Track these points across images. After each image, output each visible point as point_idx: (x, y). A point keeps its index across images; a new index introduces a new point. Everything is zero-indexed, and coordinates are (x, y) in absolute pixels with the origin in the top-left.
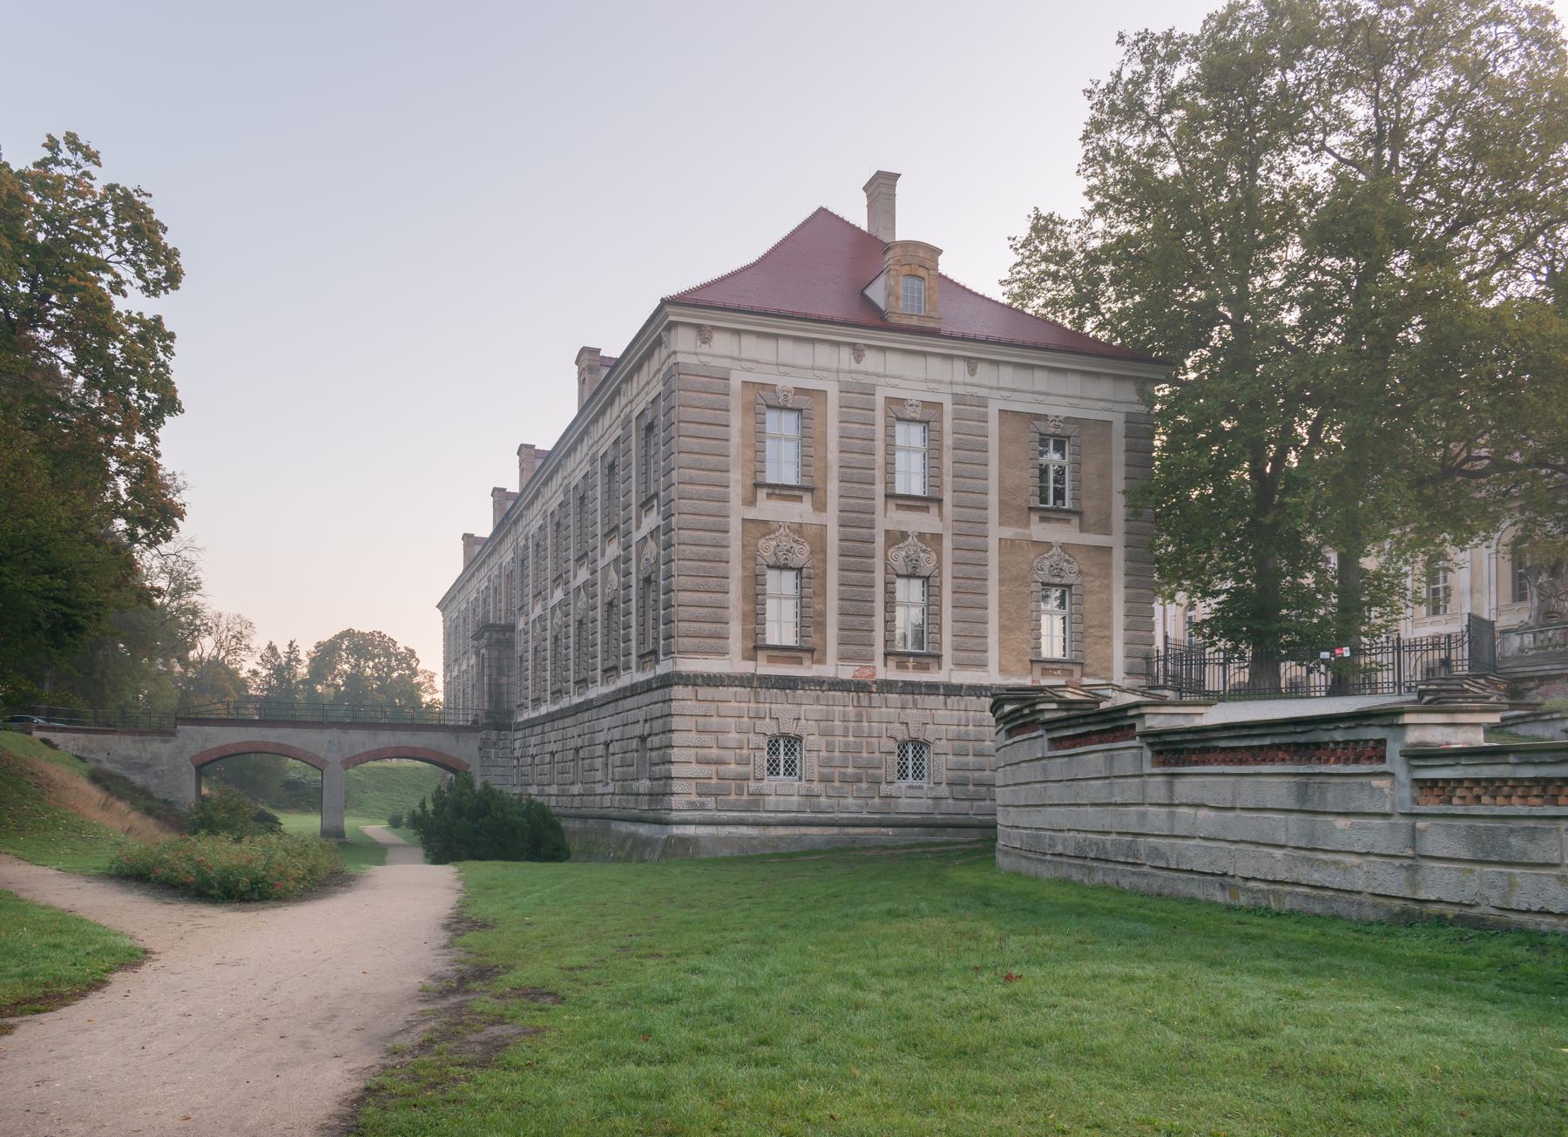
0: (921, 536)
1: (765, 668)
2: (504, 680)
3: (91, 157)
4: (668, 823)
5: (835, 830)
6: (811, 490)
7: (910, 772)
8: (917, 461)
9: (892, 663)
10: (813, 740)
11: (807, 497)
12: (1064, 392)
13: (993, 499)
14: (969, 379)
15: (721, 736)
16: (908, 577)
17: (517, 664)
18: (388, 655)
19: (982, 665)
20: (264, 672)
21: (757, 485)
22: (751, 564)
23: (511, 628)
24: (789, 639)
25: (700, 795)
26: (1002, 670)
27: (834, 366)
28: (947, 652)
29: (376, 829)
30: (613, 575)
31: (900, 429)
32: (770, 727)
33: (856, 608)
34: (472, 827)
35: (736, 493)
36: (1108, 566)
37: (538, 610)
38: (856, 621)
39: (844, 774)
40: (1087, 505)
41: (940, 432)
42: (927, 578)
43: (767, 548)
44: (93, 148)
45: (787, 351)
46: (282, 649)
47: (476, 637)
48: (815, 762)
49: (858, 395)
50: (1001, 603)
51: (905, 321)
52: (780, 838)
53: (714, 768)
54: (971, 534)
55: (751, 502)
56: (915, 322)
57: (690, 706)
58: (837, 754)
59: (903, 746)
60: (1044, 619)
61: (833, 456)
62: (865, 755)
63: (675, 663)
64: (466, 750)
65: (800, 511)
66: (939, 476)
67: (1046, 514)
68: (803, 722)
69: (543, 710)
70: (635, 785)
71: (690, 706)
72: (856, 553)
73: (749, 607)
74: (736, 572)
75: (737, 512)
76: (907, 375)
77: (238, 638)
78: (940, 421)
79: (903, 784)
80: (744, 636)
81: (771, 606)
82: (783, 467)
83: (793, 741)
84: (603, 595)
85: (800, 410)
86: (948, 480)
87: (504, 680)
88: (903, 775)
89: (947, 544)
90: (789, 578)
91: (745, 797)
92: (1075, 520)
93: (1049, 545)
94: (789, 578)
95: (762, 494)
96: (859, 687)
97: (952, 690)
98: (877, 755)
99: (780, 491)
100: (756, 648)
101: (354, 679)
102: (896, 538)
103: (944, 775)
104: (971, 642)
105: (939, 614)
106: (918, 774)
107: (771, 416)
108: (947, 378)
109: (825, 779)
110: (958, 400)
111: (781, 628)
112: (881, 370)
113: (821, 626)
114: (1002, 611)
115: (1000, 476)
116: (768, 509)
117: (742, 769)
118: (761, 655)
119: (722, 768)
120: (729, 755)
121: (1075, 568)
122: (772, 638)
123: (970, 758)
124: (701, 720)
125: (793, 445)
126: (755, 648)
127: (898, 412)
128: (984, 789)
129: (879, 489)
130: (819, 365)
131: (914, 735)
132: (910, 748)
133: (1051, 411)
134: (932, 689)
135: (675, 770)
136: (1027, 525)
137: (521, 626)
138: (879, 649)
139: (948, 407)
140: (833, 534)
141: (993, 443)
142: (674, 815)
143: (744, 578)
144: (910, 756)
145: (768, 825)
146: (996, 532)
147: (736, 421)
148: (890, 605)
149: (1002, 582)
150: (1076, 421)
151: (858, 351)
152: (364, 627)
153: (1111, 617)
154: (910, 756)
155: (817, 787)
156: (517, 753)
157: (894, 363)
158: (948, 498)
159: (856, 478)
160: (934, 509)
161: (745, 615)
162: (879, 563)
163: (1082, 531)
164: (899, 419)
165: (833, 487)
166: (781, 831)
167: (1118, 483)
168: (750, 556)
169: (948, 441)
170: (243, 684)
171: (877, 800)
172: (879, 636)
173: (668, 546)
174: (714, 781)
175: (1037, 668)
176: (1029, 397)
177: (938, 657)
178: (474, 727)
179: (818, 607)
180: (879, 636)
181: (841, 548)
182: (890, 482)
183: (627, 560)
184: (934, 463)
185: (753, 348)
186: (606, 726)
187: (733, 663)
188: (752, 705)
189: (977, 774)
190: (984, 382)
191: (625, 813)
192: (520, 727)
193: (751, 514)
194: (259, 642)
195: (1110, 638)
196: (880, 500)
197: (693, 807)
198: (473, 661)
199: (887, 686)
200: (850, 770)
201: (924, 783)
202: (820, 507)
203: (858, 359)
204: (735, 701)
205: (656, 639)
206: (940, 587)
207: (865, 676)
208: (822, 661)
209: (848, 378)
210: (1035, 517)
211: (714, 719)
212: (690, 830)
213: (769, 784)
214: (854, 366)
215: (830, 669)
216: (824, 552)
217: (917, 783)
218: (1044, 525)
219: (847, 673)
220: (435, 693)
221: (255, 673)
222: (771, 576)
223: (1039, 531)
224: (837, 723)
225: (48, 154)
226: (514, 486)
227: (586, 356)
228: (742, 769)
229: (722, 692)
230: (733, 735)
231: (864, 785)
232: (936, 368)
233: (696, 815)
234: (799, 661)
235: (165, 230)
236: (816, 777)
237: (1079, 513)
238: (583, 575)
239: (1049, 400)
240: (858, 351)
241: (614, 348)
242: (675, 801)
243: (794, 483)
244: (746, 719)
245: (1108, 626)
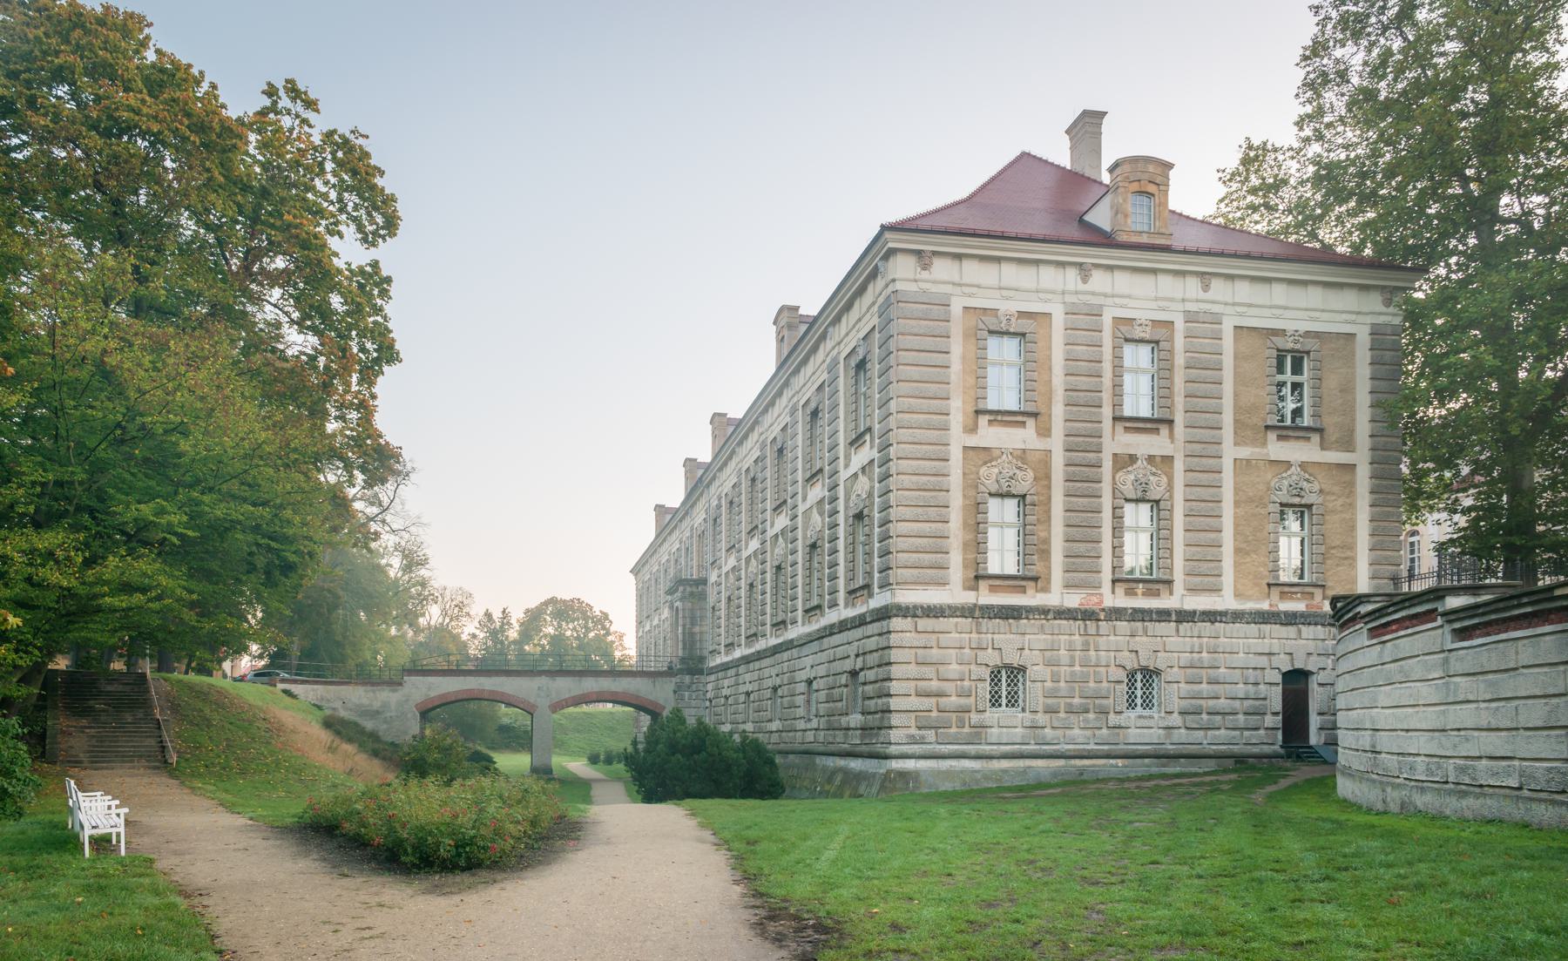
0: (1151, 459)
1: (986, 598)
2: (697, 629)
3: (311, 104)
4: (887, 757)
5: (1062, 762)
6: (1035, 415)
7: (1139, 701)
8: (1145, 383)
9: (1120, 589)
10: (1037, 671)
11: (1031, 422)
12: (1304, 305)
13: (1228, 419)
14: (1202, 295)
15: (941, 668)
16: (1137, 501)
17: (709, 614)
18: (586, 618)
19: (1216, 590)
20: (482, 635)
21: (978, 412)
22: (972, 493)
23: (704, 582)
24: (1011, 568)
25: (919, 728)
26: (1238, 595)
27: (1060, 287)
28: (1178, 576)
29: (578, 766)
30: (816, 518)
31: (1128, 350)
32: (992, 658)
33: (1082, 534)
34: (687, 764)
35: (957, 420)
36: (1350, 486)
37: (732, 562)
38: (1081, 548)
39: (1070, 705)
40: (1328, 421)
41: (1171, 351)
42: (1157, 502)
43: (989, 476)
44: (312, 96)
45: (1010, 274)
46: (497, 615)
47: (670, 592)
48: (1040, 693)
49: (1085, 317)
50: (1236, 526)
51: (1135, 239)
52: (1005, 771)
53: (933, 700)
54: (1204, 454)
55: (972, 429)
56: (1144, 239)
57: (910, 638)
58: (1062, 684)
59: (1131, 675)
60: (1283, 541)
61: (1058, 380)
62: (1092, 684)
63: (893, 595)
64: (662, 694)
65: (1024, 437)
66: (1170, 397)
67: (1284, 433)
68: (1027, 651)
69: (737, 654)
70: (844, 720)
71: (910, 638)
72: (1083, 477)
73: (970, 536)
74: (956, 500)
75: (958, 440)
76: (1133, 294)
77: (460, 606)
78: (1171, 340)
79: (1132, 714)
80: (965, 567)
81: (993, 534)
82: (1004, 392)
83: (1016, 672)
84: (805, 538)
85: (1023, 335)
86: (1179, 401)
87: (697, 629)
88: (1131, 704)
89: (1179, 466)
90: (1011, 505)
91: (967, 730)
92: (1316, 438)
93: (1288, 464)
94: (1011, 505)
95: (983, 420)
96: (1088, 615)
97: (1184, 617)
98: (1105, 684)
99: (1001, 417)
100: (978, 577)
101: (557, 640)
102: (1124, 461)
103: (1176, 704)
104: (1204, 567)
105: (1170, 538)
106: (1147, 704)
107: (993, 342)
108: (1180, 296)
109: (1050, 711)
110: (1190, 317)
111: (1002, 556)
112: (1108, 290)
113: (1045, 554)
114: (1237, 533)
115: (1236, 395)
116: (990, 436)
117: (963, 701)
118: (983, 584)
119: (942, 700)
120: (949, 687)
121: (1316, 487)
122: (993, 568)
123: (1204, 686)
124: (920, 651)
125: (1015, 371)
126: (977, 578)
127: (1126, 333)
128: (1219, 718)
129: (1107, 412)
130: (1043, 287)
131: (1144, 663)
132: (1139, 677)
133: (1290, 326)
134: (1163, 615)
135: (894, 703)
136: (1264, 444)
137: (713, 578)
138: (1107, 576)
139: (1180, 326)
141: (1228, 361)
142: (893, 749)
143: (965, 507)
144: (1139, 685)
145: (991, 757)
146: (1231, 452)
147: (957, 348)
148: (1118, 530)
149: (1237, 504)
150: (1317, 335)
151: (1084, 270)
152: (565, 595)
153: (1354, 537)
154: (1139, 685)
155: (1041, 718)
156: (709, 695)
157: (1123, 282)
158: (1179, 419)
159: (1083, 402)
160: (1164, 430)
161: (966, 545)
163: (1323, 448)
164: (1127, 340)
165: (1058, 411)
166: (1005, 764)
167: (1363, 398)
168: (971, 482)
169: (1180, 360)
170: (465, 645)
171: (1104, 731)
172: (1106, 562)
173: (886, 477)
174: (934, 714)
175: (1275, 591)
176: (1267, 312)
177: (1169, 582)
178: (670, 672)
179: (1043, 534)
180: (1106, 562)
181: (1066, 472)
182: (1117, 405)
183: (834, 500)
184: (1164, 383)
185: (974, 272)
186: (809, 664)
187: (954, 593)
188: (974, 635)
189: (1211, 703)
190: (1219, 298)
191: (832, 748)
192: (712, 671)
193: (973, 441)
194: (477, 610)
195: (1354, 559)
196: (1107, 423)
197: (913, 740)
198: (666, 613)
199: (1116, 614)
200: (1077, 701)
201: (1154, 712)
202: (1045, 432)
203: (1085, 280)
204: (956, 631)
205: (869, 574)
206: (1171, 511)
207: (1092, 603)
208: (1046, 589)
209: (1073, 299)
210: (1272, 436)
211: (935, 651)
212: (910, 764)
213: (992, 716)
214: (1081, 287)
215: (1056, 597)
216: (1048, 477)
217: (1147, 712)
218: (1281, 444)
219: (1073, 600)
220: (627, 644)
221: (474, 636)
222: (993, 505)
223: (1277, 449)
224: (1062, 652)
225: (267, 102)
226: (705, 456)
227: (786, 313)
228: (963, 701)
229: (943, 624)
230: (954, 666)
231: (1091, 716)
232: (1167, 285)
233: (916, 749)
234: (1023, 590)
235: (382, 173)
236: (1040, 708)
237: (1320, 431)
238: (782, 521)
239: (1288, 314)
240: (1084, 270)
241: (811, 308)
242: (894, 735)
243: (1015, 408)
244: (967, 651)
245: (1352, 547)
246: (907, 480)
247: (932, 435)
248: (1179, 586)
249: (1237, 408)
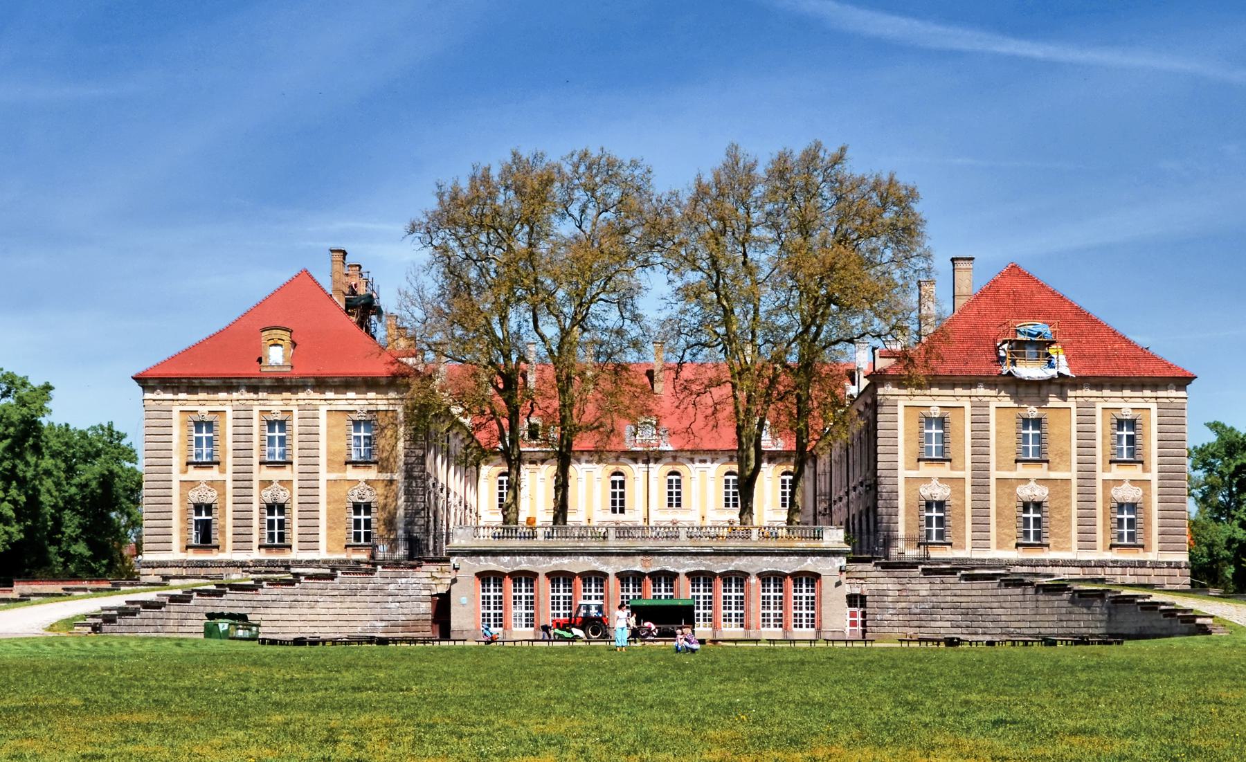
0: (280, 482)
1: (192, 556)
13: (323, 460)
26: (329, 551)
43: (194, 496)
54: (309, 478)
55: (186, 472)
65: (213, 474)
72: (243, 495)
75: (177, 477)
89: (296, 485)
93: (358, 481)
102: (266, 484)
129: (256, 460)
140: (230, 485)
141: (323, 430)
143: (181, 511)
146: (324, 475)
149: (328, 503)
158: (296, 461)
160: (288, 466)
161: (182, 530)
162: (255, 500)
168: (184, 498)
193: (185, 477)
202: (223, 471)
208: (224, 551)
210: (350, 466)
223: (352, 473)
246: (150, 500)
247: (163, 477)
248: (295, 547)
249: (329, 452)
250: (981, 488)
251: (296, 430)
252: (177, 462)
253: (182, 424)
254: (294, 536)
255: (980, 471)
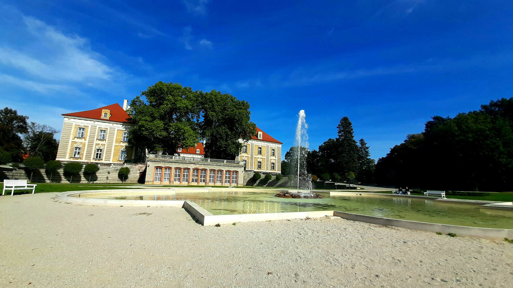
65: (83, 140)
72: (90, 146)
75: (71, 140)
102: (96, 144)
110: (110, 128)
116: (76, 140)
129: (95, 139)
146: (114, 144)
158: (107, 140)
168: (72, 145)
219: (86, 161)
250: (252, 158)
251: (108, 133)
252: (71, 137)
253: (75, 128)
254: (104, 157)
255: (252, 155)
